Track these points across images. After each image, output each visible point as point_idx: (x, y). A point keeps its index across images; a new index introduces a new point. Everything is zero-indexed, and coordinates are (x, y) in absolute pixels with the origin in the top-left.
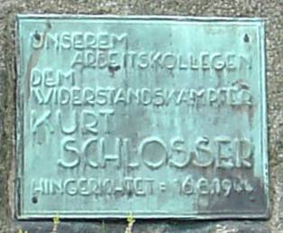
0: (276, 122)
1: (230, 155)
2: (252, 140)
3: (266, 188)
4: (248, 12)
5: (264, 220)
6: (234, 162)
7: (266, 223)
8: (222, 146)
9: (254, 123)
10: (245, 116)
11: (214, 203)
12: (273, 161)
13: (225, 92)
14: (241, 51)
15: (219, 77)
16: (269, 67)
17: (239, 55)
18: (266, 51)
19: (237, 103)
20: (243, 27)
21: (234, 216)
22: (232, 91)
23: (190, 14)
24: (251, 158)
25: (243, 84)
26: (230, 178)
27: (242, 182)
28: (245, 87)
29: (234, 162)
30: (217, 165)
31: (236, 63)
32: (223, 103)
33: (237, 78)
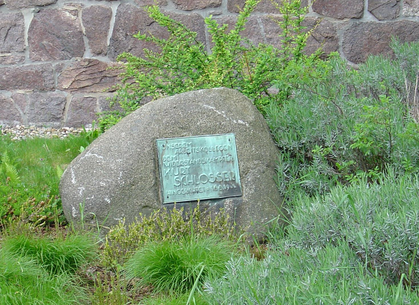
3: (240, 186)
5: (241, 196)
6: (229, 179)
7: (241, 197)
10: (231, 164)
12: (242, 178)
14: (228, 144)
20: (228, 136)
24: (234, 177)
26: (229, 184)
28: (230, 155)
29: (229, 179)
30: (224, 180)
31: (227, 148)
32: (224, 161)
33: (228, 153)
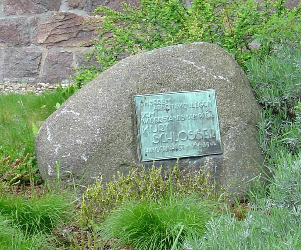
0: (222, 122)
1: (208, 134)
2: (214, 129)
3: (221, 144)
4: (209, 87)
5: (221, 154)
6: (209, 136)
7: (222, 155)
8: (205, 131)
9: (215, 123)
10: (212, 121)
11: (204, 150)
12: (222, 135)
13: (204, 114)
14: (208, 100)
15: (202, 109)
16: (218, 105)
17: (208, 102)
18: (216, 99)
19: (208, 117)
20: (208, 92)
21: (211, 154)
22: (206, 113)
23: (190, 90)
24: (215, 135)
25: (210, 111)
26: (209, 141)
27: (213, 143)
28: (210, 112)
29: (209, 136)
30: (204, 138)
31: (207, 104)
32: (204, 117)
33: (208, 109)
